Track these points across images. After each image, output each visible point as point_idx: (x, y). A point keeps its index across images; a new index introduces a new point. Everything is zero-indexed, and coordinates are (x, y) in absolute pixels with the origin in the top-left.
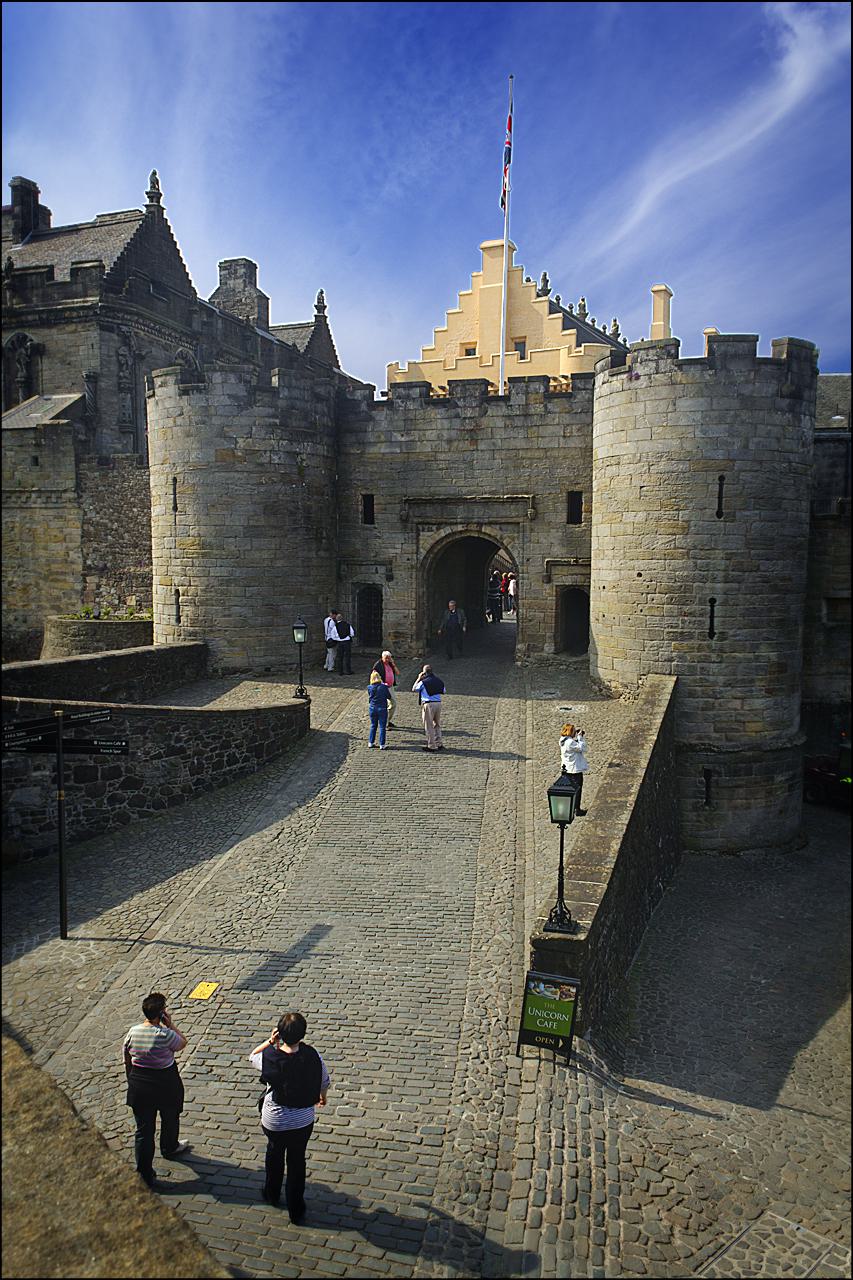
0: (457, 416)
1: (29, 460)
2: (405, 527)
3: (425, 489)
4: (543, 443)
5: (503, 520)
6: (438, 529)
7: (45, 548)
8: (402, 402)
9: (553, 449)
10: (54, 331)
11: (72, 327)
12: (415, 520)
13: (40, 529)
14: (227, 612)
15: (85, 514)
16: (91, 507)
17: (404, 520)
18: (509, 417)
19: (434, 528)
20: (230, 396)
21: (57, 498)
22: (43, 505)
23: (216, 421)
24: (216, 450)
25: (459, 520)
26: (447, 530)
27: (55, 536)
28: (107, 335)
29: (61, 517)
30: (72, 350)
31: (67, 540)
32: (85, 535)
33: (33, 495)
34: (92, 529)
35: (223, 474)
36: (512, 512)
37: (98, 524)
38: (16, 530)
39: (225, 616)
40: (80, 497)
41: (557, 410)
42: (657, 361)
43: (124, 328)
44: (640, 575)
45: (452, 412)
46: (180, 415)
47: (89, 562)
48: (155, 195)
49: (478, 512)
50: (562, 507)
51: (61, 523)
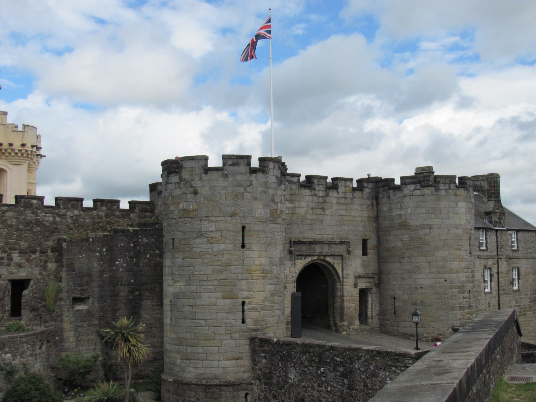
0: (316, 195)
2: (291, 257)
3: (301, 235)
4: (353, 213)
5: (337, 254)
6: (305, 259)
8: (289, 184)
9: (357, 216)
12: (297, 253)
14: (273, 314)
17: (290, 252)
18: (338, 198)
19: (303, 258)
20: (276, 177)
23: (271, 191)
24: (271, 210)
25: (317, 253)
26: (309, 260)
35: (273, 225)
36: (341, 249)
39: (273, 317)
41: (358, 197)
42: (449, 184)
44: (446, 281)
45: (313, 192)
46: (250, 186)
49: (326, 249)
50: (360, 247)
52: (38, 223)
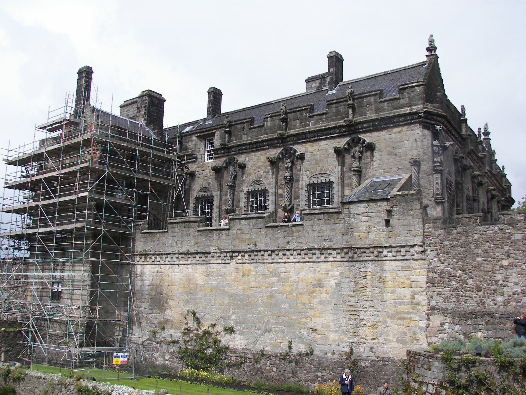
1: (383, 223)
7: (393, 292)
10: (383, 133)
11: (399, 129)
13: (388, 276)
15: (431, 264)
16: (435, 259)
21: (406, 251)
22: (394, 258)
27: (403, 283)
28: (426, 132)
29: (409, 267)
30: (398, 144)
31: (413, 285)
32: (430, 281)
33: (385, 251)
34: (436, 276)
37: (442, 272)
38: (369, 278)
40: (424, 252)
43: (438, 127)
47: (433, 303)
48: (432, 49)
51: (407, 272)
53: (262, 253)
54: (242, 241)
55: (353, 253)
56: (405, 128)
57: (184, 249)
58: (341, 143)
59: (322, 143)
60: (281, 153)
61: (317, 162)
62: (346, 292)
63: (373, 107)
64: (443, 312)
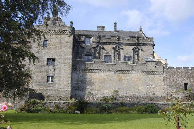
10: (144, 47)
11: (148, 47)
32: (164, 79)
37: (167, 77)
47: (165, 84)
52: (189, 72)
53: (125, 71)
54: (120, 68)
55: (148, 73)
56: (149, 47)
57: (101, 68)
58: (133, 47)
59: (128, 46)
60: (115, 47)
61: (127, 51)
62: (147, 81)
63: (142, 40)
64: (167, 85)
